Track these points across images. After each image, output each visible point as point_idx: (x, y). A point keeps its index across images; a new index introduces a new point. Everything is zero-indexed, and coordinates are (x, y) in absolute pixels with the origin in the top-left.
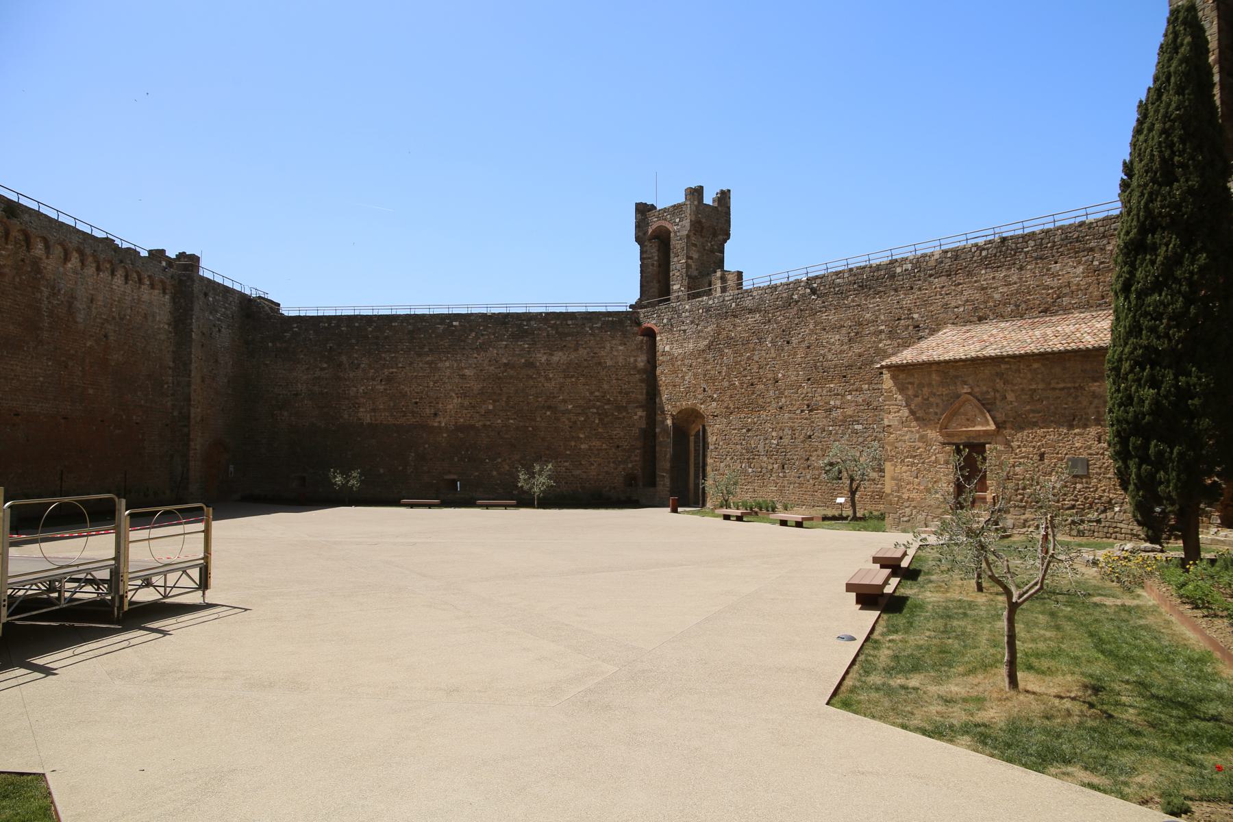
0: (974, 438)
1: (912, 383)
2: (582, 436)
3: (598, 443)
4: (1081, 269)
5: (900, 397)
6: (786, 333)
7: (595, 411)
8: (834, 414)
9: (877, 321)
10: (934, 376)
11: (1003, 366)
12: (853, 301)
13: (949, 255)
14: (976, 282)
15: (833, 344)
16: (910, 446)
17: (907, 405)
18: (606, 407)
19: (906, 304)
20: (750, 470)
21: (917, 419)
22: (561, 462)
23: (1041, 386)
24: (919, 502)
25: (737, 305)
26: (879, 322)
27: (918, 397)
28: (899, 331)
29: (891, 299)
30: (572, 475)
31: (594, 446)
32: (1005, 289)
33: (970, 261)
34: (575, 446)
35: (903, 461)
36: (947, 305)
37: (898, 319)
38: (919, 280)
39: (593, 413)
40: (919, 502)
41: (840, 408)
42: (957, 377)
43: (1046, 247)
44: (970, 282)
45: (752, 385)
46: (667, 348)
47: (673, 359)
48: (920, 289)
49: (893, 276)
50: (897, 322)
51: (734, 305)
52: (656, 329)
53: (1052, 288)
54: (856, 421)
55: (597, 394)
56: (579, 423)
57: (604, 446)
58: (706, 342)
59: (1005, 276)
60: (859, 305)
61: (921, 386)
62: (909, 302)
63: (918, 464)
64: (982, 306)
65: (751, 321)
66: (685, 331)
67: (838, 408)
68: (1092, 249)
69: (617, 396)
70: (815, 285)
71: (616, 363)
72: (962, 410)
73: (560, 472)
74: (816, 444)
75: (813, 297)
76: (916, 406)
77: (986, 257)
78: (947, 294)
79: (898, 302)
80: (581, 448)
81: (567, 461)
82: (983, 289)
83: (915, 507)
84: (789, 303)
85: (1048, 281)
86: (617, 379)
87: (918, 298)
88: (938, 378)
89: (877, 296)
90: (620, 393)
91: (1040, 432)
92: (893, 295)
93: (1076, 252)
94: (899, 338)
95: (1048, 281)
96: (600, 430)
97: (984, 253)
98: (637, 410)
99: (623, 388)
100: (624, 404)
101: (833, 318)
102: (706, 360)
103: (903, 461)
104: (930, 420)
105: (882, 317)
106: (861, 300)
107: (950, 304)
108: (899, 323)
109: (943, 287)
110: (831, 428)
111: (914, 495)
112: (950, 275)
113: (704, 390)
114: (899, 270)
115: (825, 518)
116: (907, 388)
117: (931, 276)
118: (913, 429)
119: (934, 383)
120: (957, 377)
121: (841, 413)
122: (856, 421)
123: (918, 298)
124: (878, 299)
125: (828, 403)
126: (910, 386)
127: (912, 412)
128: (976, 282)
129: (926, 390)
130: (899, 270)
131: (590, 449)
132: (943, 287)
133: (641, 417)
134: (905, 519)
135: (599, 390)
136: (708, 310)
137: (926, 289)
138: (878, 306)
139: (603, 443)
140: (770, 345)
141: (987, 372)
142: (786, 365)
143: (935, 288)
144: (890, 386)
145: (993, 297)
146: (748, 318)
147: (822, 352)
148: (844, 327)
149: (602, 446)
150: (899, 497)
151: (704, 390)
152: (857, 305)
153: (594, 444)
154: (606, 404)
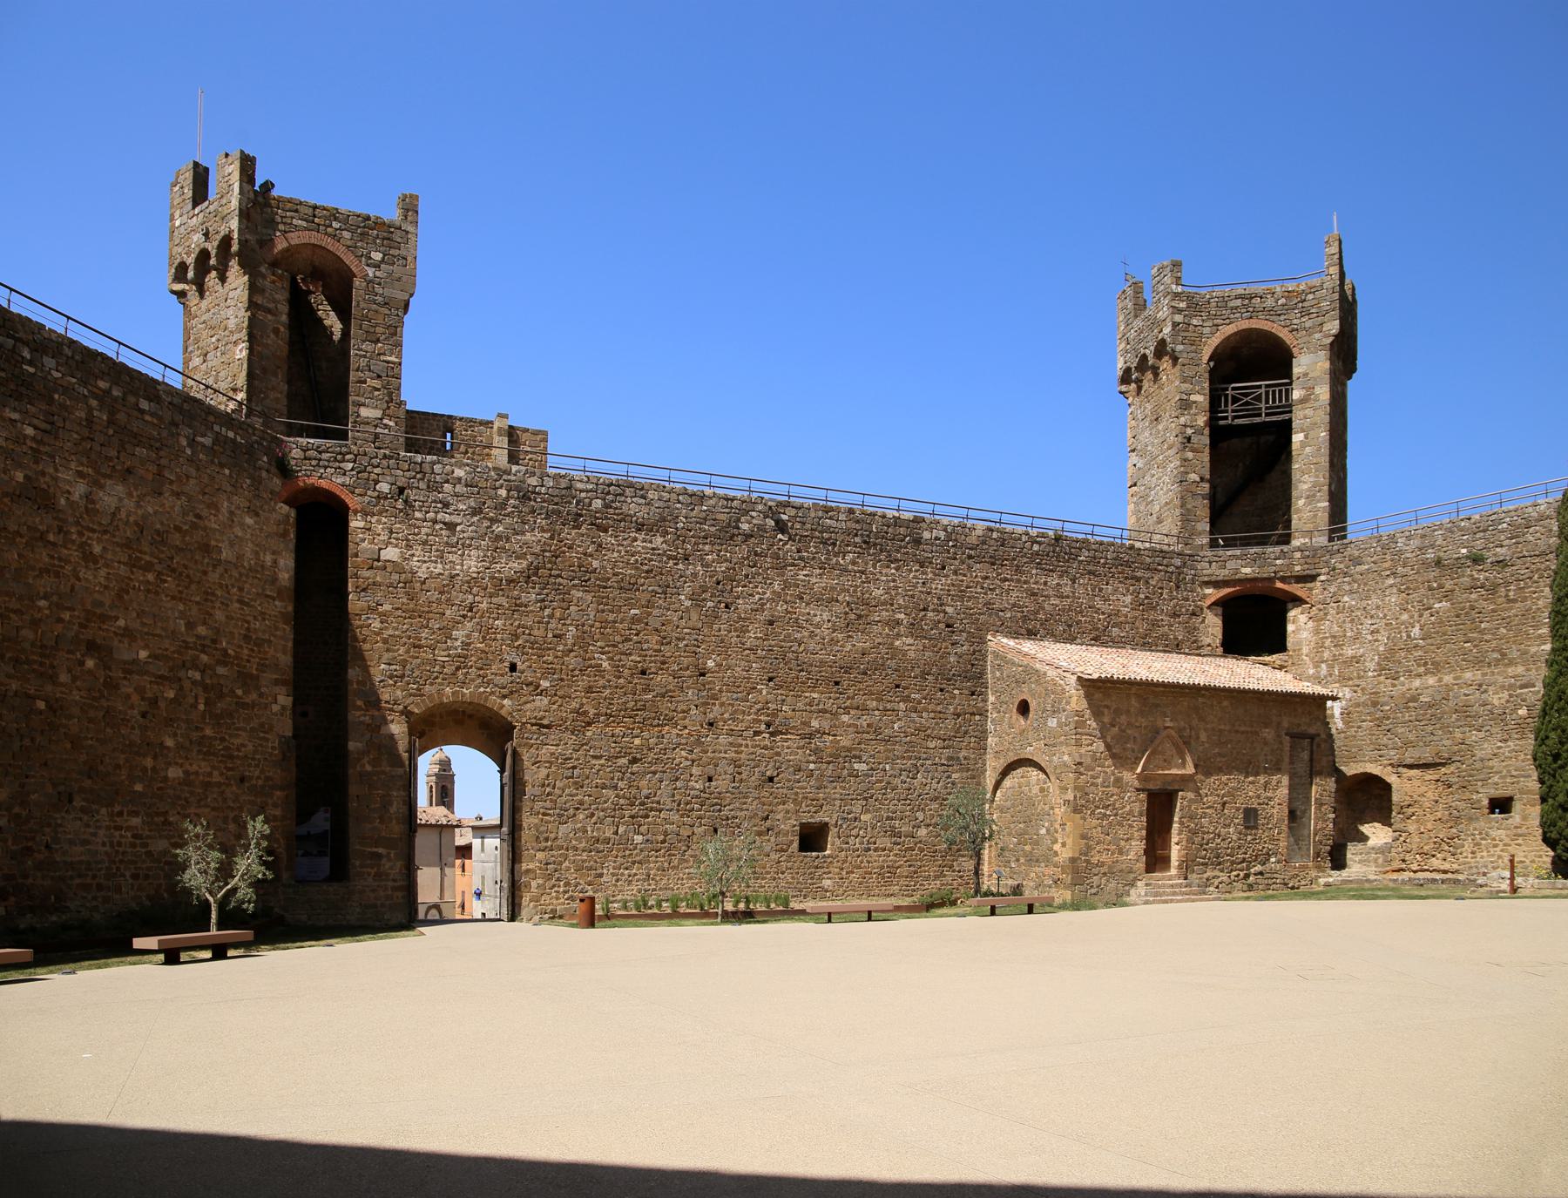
0: (1169, 784)
1: (1108, 707)
2: (170, 743)
3: (205, 767)
4: (1128, 599)
5: (1094, 725)
6: (723, 588)
7: (197, 676)
8: (816, 742)
9: (892, 605)
10: (1134, 702)
11: (1200, 700)
12: (854, 563)
13: (995, 535)
14: (1025, 582)
15: (818, 626)
16: (1103, 792)
17: (1103, 737)
18: (221, 670)
19: (936, 589)
20: (638, 839)
21: (1113, 756)
22: (120, 814)
23: (1227, 728)
24: (1110, 867)
25: (607, 506)
26: (896, 606)
27: (1114, 726)
28: (926, 627)
29: (913, 574)
30: (149, 854)
31: (197, 773)
32: (1057, 602)
33: (1020, 552)
34: (154, 769)
35: (1093, 813)
36: (990, 604)
37: (924, 609)
38: (955, 559)
39: (194, 683)
40: (1110, 867)
41: (829, 734)
42: (1157, 706)
43: (1099, 562)
44: (1018, 581)
45: (643, 672)
46: (391, 554)
47: (408, 581)
48: (955, 573)
49: (917, 542)
50: (923, 613)
51: (597, 504)
52: (352, 501)
53: (1103, 613)
54: (855, 757)
55: (201, 630)
56: (162, 704)
57: (216, 777)
58: (517, 565)
59: (1058, 584)
60: (862, 572)
61: (1117, 712)
62: (940, 586)
63: (1110, 816)
64: (1032, 617)
65: (643, 548)
66: (451, 527)
67: (824, 733)
68: (1138, 579)
69: (240, 647)
70: (785, 517)
71: (240, 557)
72: (1160, 748)
73: (119, 844)
74: (785, 791)
75: (780, 536)
76: (1112, 738)
77: (1037, 553)
78: (990, 590)
79: (923, 583)
80: (166, 779)
81: (136, 814)
82: (1034, 594)
83: (1105, 874)
84: (728, 534)
85: (1098, 603)
86: (241, 602)
87: (953, 585)
88: (1137, 705)
89: (893, 565)
90: (247, 638)
91: (1224, 778)
92: (916, 571)
93: (1126, 578)
94: (926, 638)
95: (1098, 603)
96: (208, 732)
97: (1036, 547)
98: (277, 689)
99: (252, 626)
100: (254, 672)
101: (819, 583)
102: (518, 606)
103: (1093, 813)
104: (1127, 758)
105: (901, 601)
106: (867, 564)
107: (994, 604)
108: (925, 615)
109: (987, 578)
110: (812, 766)
111: (1104, 858)
112: (993, 564)
113: (513, 668)
114: (926, 535)
115: (898, 909)
116: (1103, 714)
117: (970, 557)
118: (1108, 770)
119: (1132, 710)
120: (1157, 706)
121: (831, 742)
122: (855, 757)
123: (953, 585)
124: (893, 571)
125: (806, 724)
126: (1106, 711)
127: (1108, 747)
128: (1025, 582)
129: (1123, 719)
130: (926, 535)
131: (186, 781)
132: (987, 578)
133: (284, 708)
134: (1093, 891)
135: (204, 623)
136: (525, 496)
137: (965, 575)
138: (894, 581)
139: (213, 767)
140: (688, 603)
141: (1185, 704)
142: (723, 647)
143: (976, 576)
144: (1083, 707)
145: (1044, 608)
146: (635, 540)
147: (798, 635)
148: (837, 601)
149: (210, 774)
150: (1088, 862)
151: (513, 668)
152: (859, 572)
153: (195, 768)
154: (219, 662)
